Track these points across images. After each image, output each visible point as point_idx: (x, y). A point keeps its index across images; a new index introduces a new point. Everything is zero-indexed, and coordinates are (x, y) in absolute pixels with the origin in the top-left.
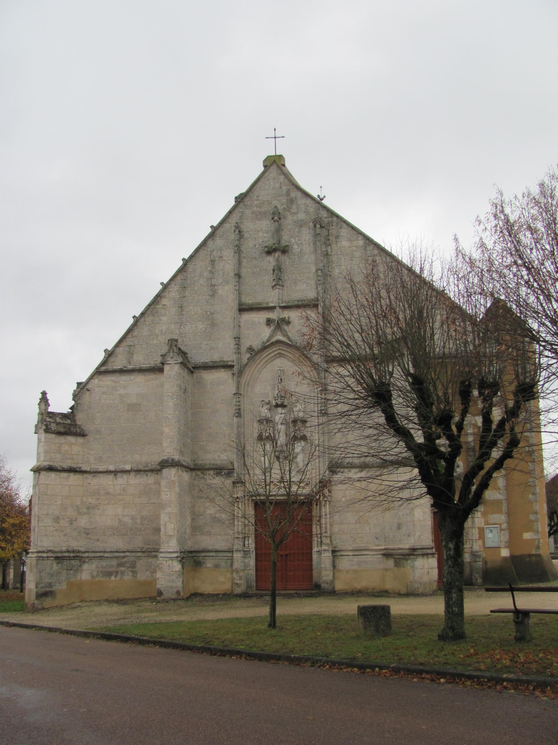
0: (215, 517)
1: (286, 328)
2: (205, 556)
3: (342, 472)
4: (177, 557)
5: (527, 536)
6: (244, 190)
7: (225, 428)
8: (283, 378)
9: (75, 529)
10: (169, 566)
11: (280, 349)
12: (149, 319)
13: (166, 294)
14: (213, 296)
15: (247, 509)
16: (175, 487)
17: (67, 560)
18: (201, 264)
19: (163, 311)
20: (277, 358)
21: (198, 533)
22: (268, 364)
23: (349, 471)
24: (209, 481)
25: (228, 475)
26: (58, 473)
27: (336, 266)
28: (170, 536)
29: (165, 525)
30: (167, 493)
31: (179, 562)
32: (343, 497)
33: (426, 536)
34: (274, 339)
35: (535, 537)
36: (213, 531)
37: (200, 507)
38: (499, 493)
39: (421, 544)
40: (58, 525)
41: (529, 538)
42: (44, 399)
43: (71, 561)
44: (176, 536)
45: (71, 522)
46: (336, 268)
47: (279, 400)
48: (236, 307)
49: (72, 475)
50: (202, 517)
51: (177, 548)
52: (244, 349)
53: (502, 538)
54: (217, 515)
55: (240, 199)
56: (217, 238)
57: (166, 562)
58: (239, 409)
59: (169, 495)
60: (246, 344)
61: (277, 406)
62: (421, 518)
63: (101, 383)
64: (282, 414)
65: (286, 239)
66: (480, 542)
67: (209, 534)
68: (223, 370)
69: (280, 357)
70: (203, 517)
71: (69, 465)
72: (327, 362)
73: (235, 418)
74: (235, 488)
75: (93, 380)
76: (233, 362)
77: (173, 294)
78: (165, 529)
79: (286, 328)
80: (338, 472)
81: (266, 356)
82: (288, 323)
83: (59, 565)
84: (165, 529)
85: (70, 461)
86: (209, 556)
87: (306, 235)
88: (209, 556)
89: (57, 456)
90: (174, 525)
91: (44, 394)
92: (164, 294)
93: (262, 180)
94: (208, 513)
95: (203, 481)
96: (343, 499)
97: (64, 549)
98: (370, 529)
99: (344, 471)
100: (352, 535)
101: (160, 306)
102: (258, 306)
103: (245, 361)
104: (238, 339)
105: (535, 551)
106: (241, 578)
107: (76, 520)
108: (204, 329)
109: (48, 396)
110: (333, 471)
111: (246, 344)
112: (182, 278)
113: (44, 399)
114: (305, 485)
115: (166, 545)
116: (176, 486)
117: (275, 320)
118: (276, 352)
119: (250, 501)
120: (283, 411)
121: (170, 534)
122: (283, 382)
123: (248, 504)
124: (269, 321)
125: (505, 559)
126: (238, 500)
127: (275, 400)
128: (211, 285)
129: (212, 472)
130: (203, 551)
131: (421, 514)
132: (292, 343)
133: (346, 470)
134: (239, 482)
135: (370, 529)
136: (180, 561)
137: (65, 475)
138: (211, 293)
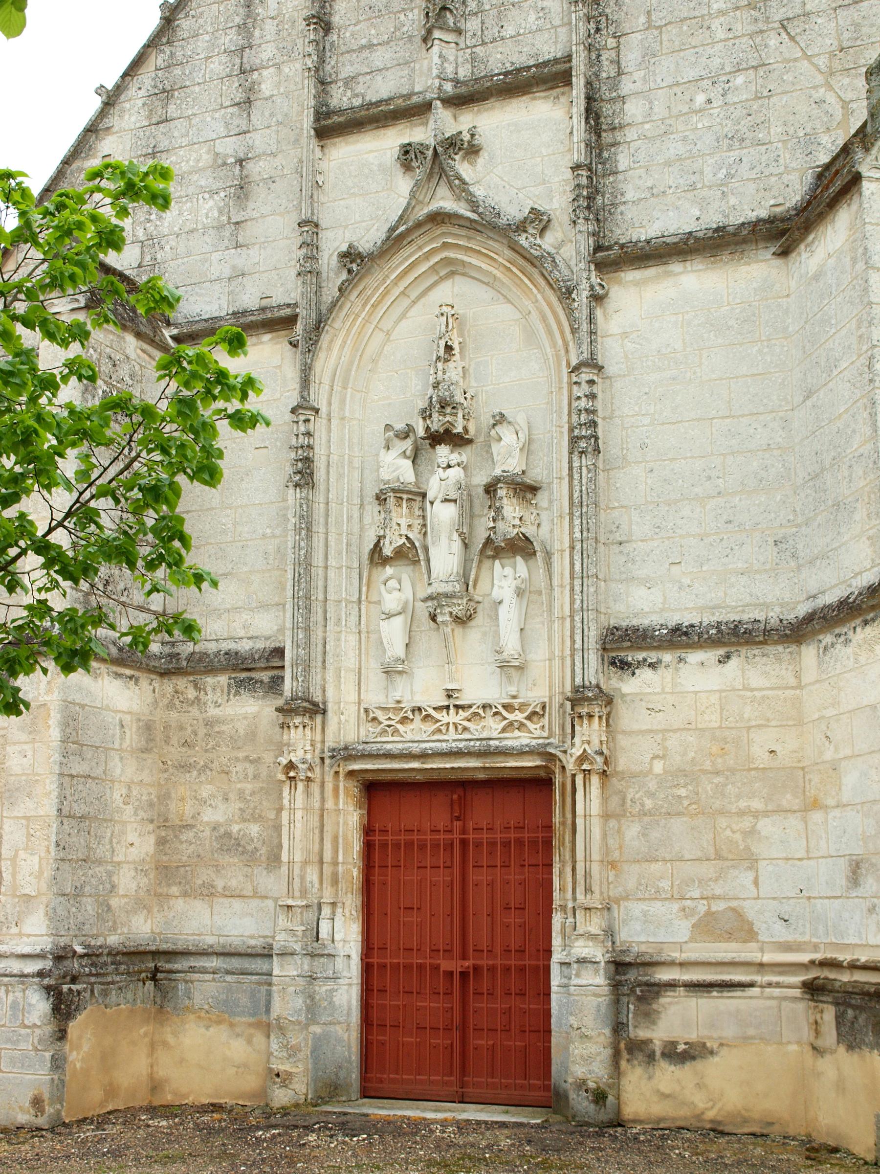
0: (228, 835)
1: (464, 168)
2: (192, 969)
3: (652, 666)
4: (41, 974)
7: (268, 531)
8: (456, 346)
10: (14, 1006)
11: (445, 245)
13: (114, 120)
15: (330, 804)
16: (49, 727)
20: (442, 279)
21: (175, 890)
22: (414, 302)
23: (681, 660)
24: (213, 712)
25: (271, 688)
28: (28, 898)
29: (14, 860)
30: (25, 747)
31: (43, 992)
32: (655, 757)
34: (422, 212)
36: (220, 884)
37: (182, 799)
44: (44, 899)
47: (435, 416)
48: (307, 121)
50: (188, 835)
51: (45, 943)
52: (328, 259)
54: (235, 828)
57: (7, 992)
58: (308, 461)
59: (30, 753)
61: (435, 439)
64: (449, 466)
67: (208, 893)
68: (267, 337)
69: (452, 273)
70: (191, 834)
72: (602, 266)
73: (291, 491)
74: (286, 729)
76: (296, 305)
77: (133, 119)
78: (14, 875)
79: (464, 168)
80: (640, 664)
81: (401, 277)
82: (473, 151)
84: (14, 875)
86: (204, 971)
88: (204, 971)
90: (41, 859)
92: (107, 122)
94: (206, 819)
95: (195, 711)
96: (658, 767)
98: (756, 883)
99: (659, 661)
102: (374, 111)
103: (330, 292)
106: (292, 1052)
108: (216, 214)
110: (621, 661)
112: (160, 62)
114: (529, 718)
115: (14, 930)
116: (50, 723)
117: (427, 147)
118: (436, 259)
119: (341, 776)
120: (455, 458)
121: (27, 891)
122: (457, 357)
123: (336, 789)
124: (407, 152)
126: (292, 774)
127: (424, 419)
128: (243, 72)
129: (223, 679)
130: (186, 954)
132: (480, 214)
133: (667, 657)
135: (756, 883)
136: (48, 989)
138: (239, 96)
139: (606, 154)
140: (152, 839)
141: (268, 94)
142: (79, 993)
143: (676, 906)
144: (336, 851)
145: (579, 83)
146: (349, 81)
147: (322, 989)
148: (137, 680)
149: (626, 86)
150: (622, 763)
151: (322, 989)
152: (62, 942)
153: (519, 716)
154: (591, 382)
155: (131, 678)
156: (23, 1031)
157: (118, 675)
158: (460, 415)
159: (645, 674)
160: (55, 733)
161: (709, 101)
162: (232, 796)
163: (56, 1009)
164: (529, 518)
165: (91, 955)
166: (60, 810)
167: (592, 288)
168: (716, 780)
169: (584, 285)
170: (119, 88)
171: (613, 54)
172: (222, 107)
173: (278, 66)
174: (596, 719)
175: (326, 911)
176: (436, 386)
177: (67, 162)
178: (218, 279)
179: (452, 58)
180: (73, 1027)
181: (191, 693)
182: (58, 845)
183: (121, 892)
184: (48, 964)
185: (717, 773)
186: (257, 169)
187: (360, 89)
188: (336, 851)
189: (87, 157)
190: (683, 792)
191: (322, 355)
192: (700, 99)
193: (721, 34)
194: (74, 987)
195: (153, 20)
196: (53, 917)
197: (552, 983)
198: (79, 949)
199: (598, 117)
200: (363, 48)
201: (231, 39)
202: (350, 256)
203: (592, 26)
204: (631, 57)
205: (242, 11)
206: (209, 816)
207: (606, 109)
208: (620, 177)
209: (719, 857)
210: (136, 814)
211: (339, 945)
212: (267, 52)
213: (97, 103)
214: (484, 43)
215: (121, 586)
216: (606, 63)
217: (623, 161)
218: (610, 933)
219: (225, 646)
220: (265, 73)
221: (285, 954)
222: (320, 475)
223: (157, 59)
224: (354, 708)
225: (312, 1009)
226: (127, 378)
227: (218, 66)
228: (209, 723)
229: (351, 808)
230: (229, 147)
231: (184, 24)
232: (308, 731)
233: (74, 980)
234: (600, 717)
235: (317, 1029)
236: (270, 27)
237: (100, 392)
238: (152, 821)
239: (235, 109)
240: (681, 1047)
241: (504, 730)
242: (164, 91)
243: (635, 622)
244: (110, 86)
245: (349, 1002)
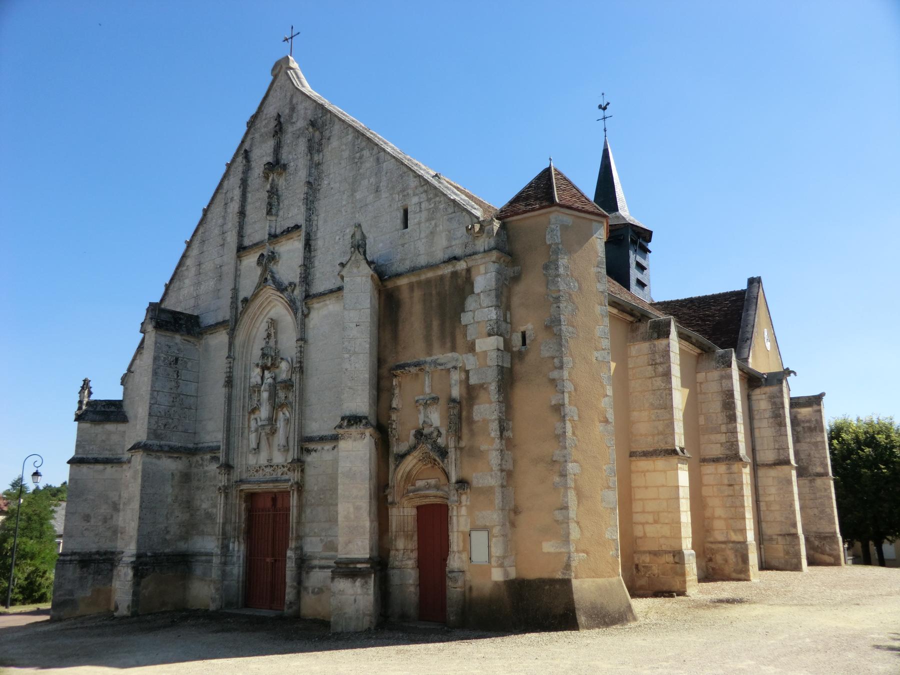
0: (208, 512)
3: (315, 451)
4: (132, 562)
5: (548, 547)
6: (253, 111)
8: (273, 334)
9: (109, 528)
10: (125, 574)
12: (176, 284)
14: (223, 245)
17: (95, 563)
18: (217, 209)
19: (186, 273)
24: (206, 468)
26: (91, 466)
27: (325, 176)
28: (131, 537)
33: (360, 543)
35: (563, 550)
36: (205, 530)
38: (491, 476)
39: (348, 556)
40: (88, 524)
41: (552, 550)
42: (86, 385)
43: (100, 565)
45: (105, 520)
46: (325, 178)
49: (109, 467)
51: (134, 552)
53: (493, 549)
54: (210, 510)
55: (252, 123)
56: (232, 176)
60: (242, 295)
62: (352, 516)
63: (142, 363)
65: (285, 156)
66: (464, 556)
71: (107, 456)
75: (136, 361)
83: (85, 570)
85: (107, 452)
87: (302, 146)
89: (91, 448)
91: (86, 383)
93: (272, 92)
96: (316, 489)
97: (94, 550)
100: (322, 538)
101: (185, 268)
104: (235, 290)
105: (563, 574)
106: (217, 590)
107: (112, 517)
109: (91, 384)
111: (241, 298)
113: (86, 385)
125: (496, 583)
128: (223, 233)
131: (352, 510)
134: (228, 467)
137: (100, 467)
138: (221, 242)
139: (312, 260)
140: (188, 514)
141: (229, 241)
142: (147, 569)
143: (319, 538)
144: (236, 518)
145: (303, 234)
146: (249, 235)
147: (228, 568)
148: (180, 458)
149: (319, 235)
150: (307, 487)
151: (228, 568)
152: (142, 551)
153: (286, 469)
154: (301, 347)
155: (177, 458)
156: (127, 583)
157: (170, 457)
158: (270, 359)
159: (313, 454)
160: (139, 480)
161: (340, 239)
162: (210, 499)
163: (135, 575)
164: (290, 395)
165: (155, 556)
166: (141, 506)
167: (303, 311)
168: (331, 493)
169: (300, 311)
170: (191, 240)
171: (316, 222)
172: (217, 247)
173: (231, 231)
174: (296, 471)
175: (232, 540)
176: (262, 349)
177: (177, 268)
178: (213, 311)
179: (274, 226)
180: (144, 582)
181: (200, 462)
182: (140, 518)
183: (172, 534)
184: (133, 559)
185: (331, 490)
186: (224, 268)
187: (252, 239)
188: (236, 518)
189: (184, 266)
190: (322, 497)
191: (237, 338)
192: (337, 238)
193: (344, 213)
194: (144, 567)
195: (200, 215)
196: (139, 543)
197: (287, 566)
198: (149, 554)
199: (310, 245)
200: (253, 223)
201: (220, 221)
202: (245, 301)
203: (311, 212)
204: (320, 223)
205: (224, 210)
206: (204, 506)
207: (312, 243)
208: (316, 268)
209: (330, 521)
210: (180, 506)
211: (236, 552)
212: (229, 225)
213: (184, 246)
214: (284, 220)
215: (173, 425)
216: (314, 226)
217: (317, 263)
218: (299, 548)
219: (211, 444)
220: (229, 233)
221: (217, 555)
222: (234, 383)
223: (201, 230)
224: (244, 466)
225: (224, 575)
226: (176, 351)
227: (216, 231)
228: (205, 472)
229: (243, 503)
230: (218, 261)
231: (209, 216)
232: (226, 475)
233: (146, 564)
234: (298, 471)
235: (226, 583)
236: (231, 216)
237: (162, 358)
238: (189, 508)
239: (220, 247)
240: (316, 590)
241: (282, 474)
242: (204, 241)
243: (312, 435)
244: (188, 241)
245: (239, 572)
